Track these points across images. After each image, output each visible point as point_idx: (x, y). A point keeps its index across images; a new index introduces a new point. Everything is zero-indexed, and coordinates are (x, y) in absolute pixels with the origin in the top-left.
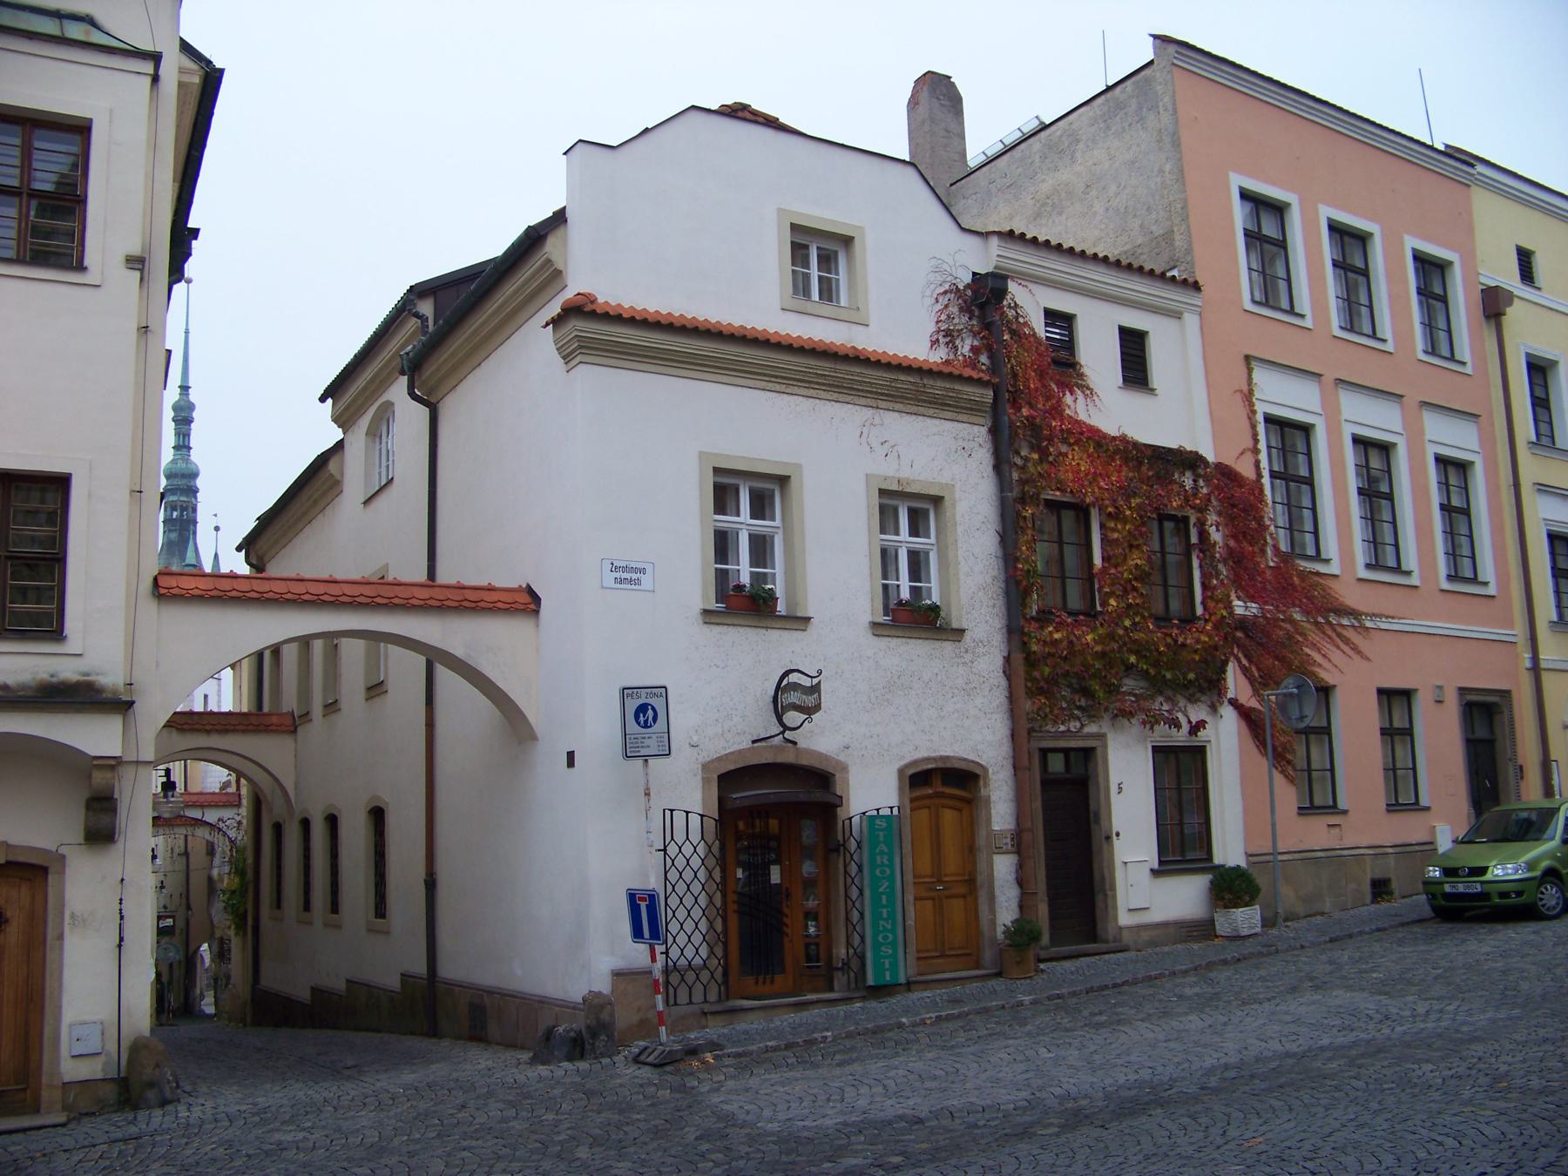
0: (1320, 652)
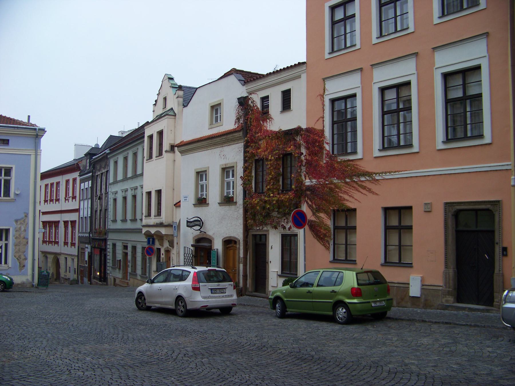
0: (348, 195)
